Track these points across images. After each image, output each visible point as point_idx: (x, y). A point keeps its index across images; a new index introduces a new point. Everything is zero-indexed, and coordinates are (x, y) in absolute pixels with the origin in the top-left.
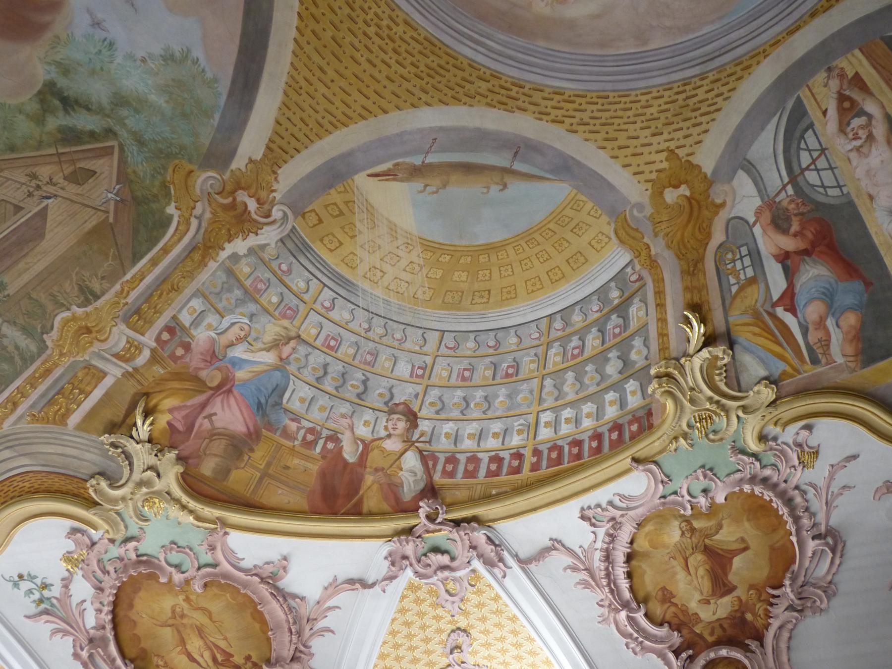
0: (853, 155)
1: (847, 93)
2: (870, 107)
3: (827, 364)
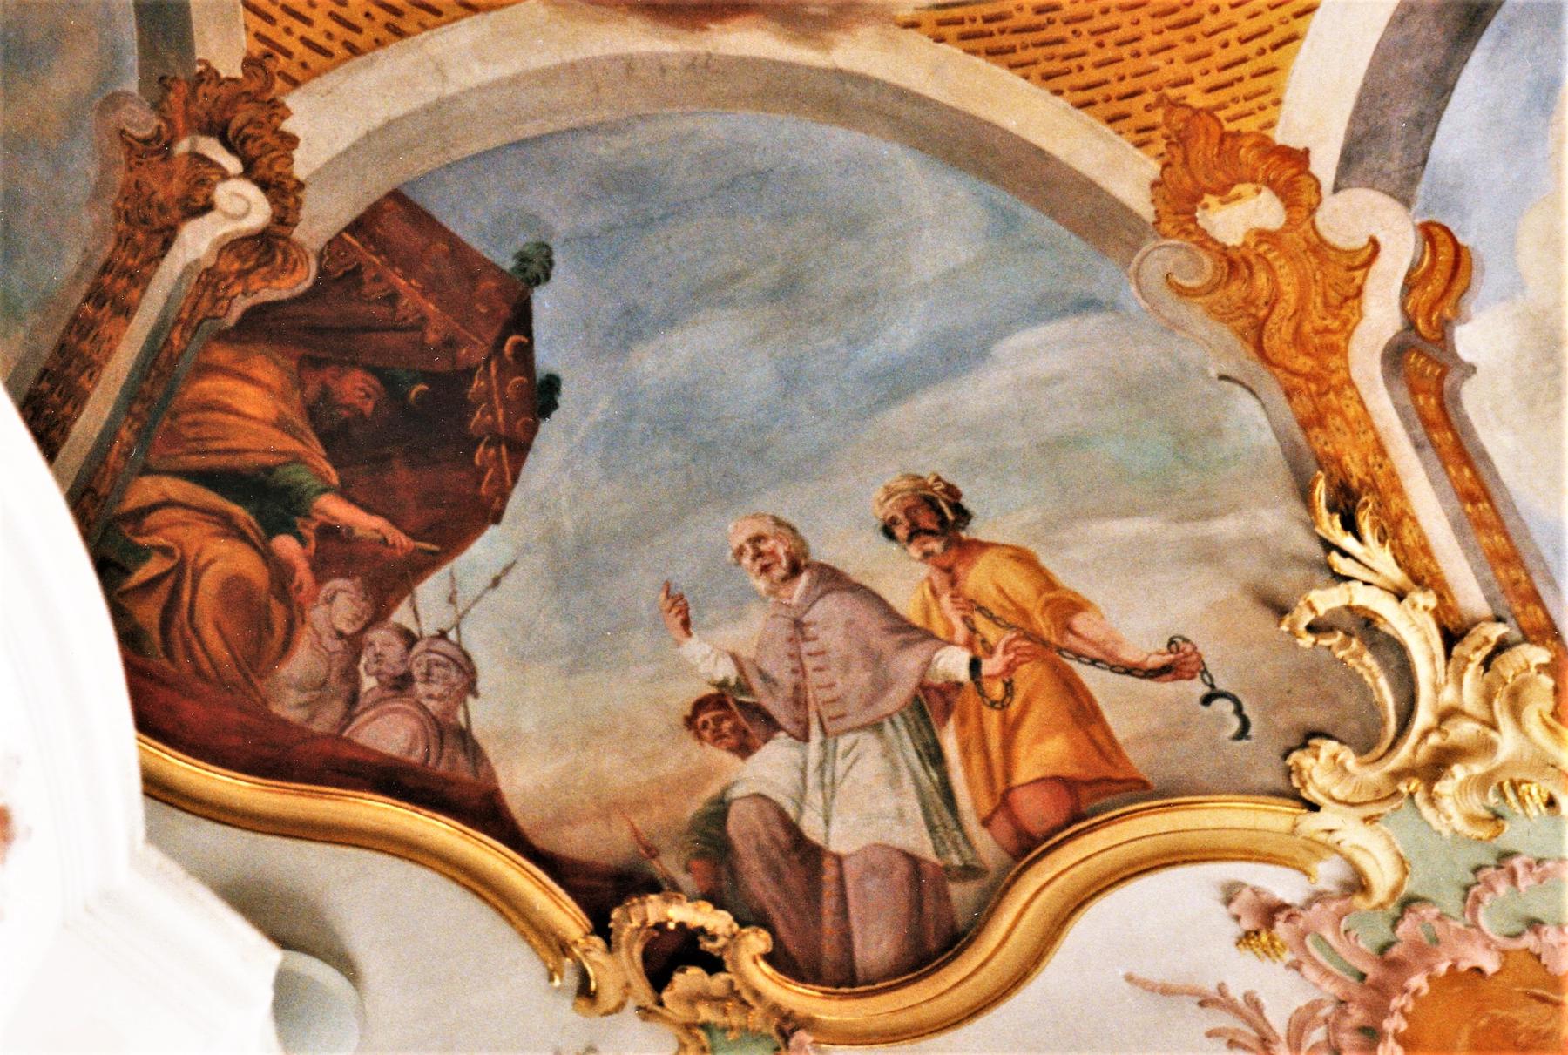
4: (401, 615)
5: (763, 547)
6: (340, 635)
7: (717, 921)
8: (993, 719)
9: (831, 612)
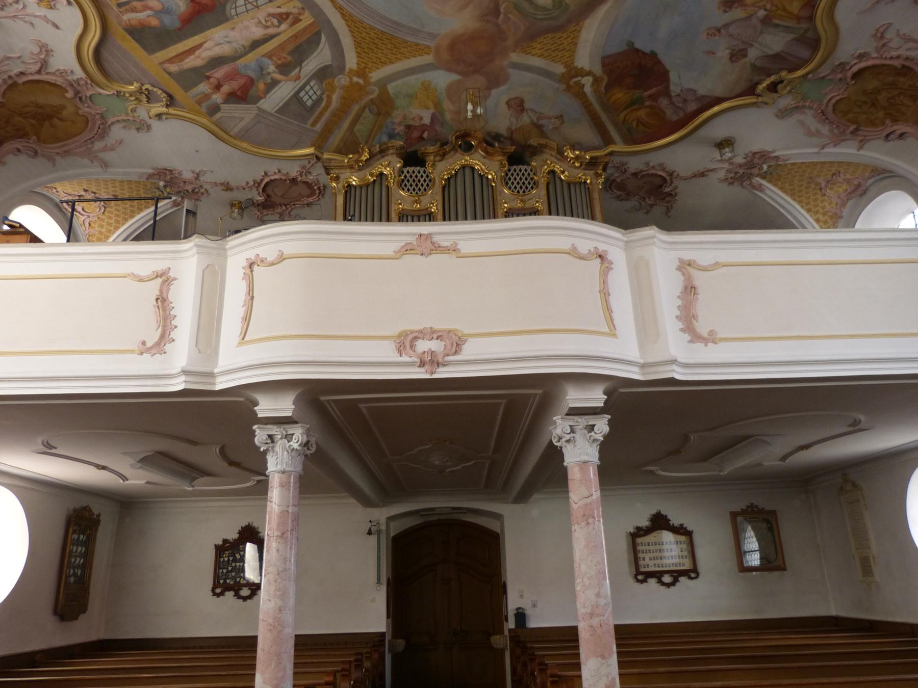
0: (256, 20)
1: (291, 16)
2: (284, 27)
3: (120, 12)
4: (673, 94)
5: (710, 34)
6: (669, 104)
7: (773, 78)
8: (779, 12)
9: (732, 30)
